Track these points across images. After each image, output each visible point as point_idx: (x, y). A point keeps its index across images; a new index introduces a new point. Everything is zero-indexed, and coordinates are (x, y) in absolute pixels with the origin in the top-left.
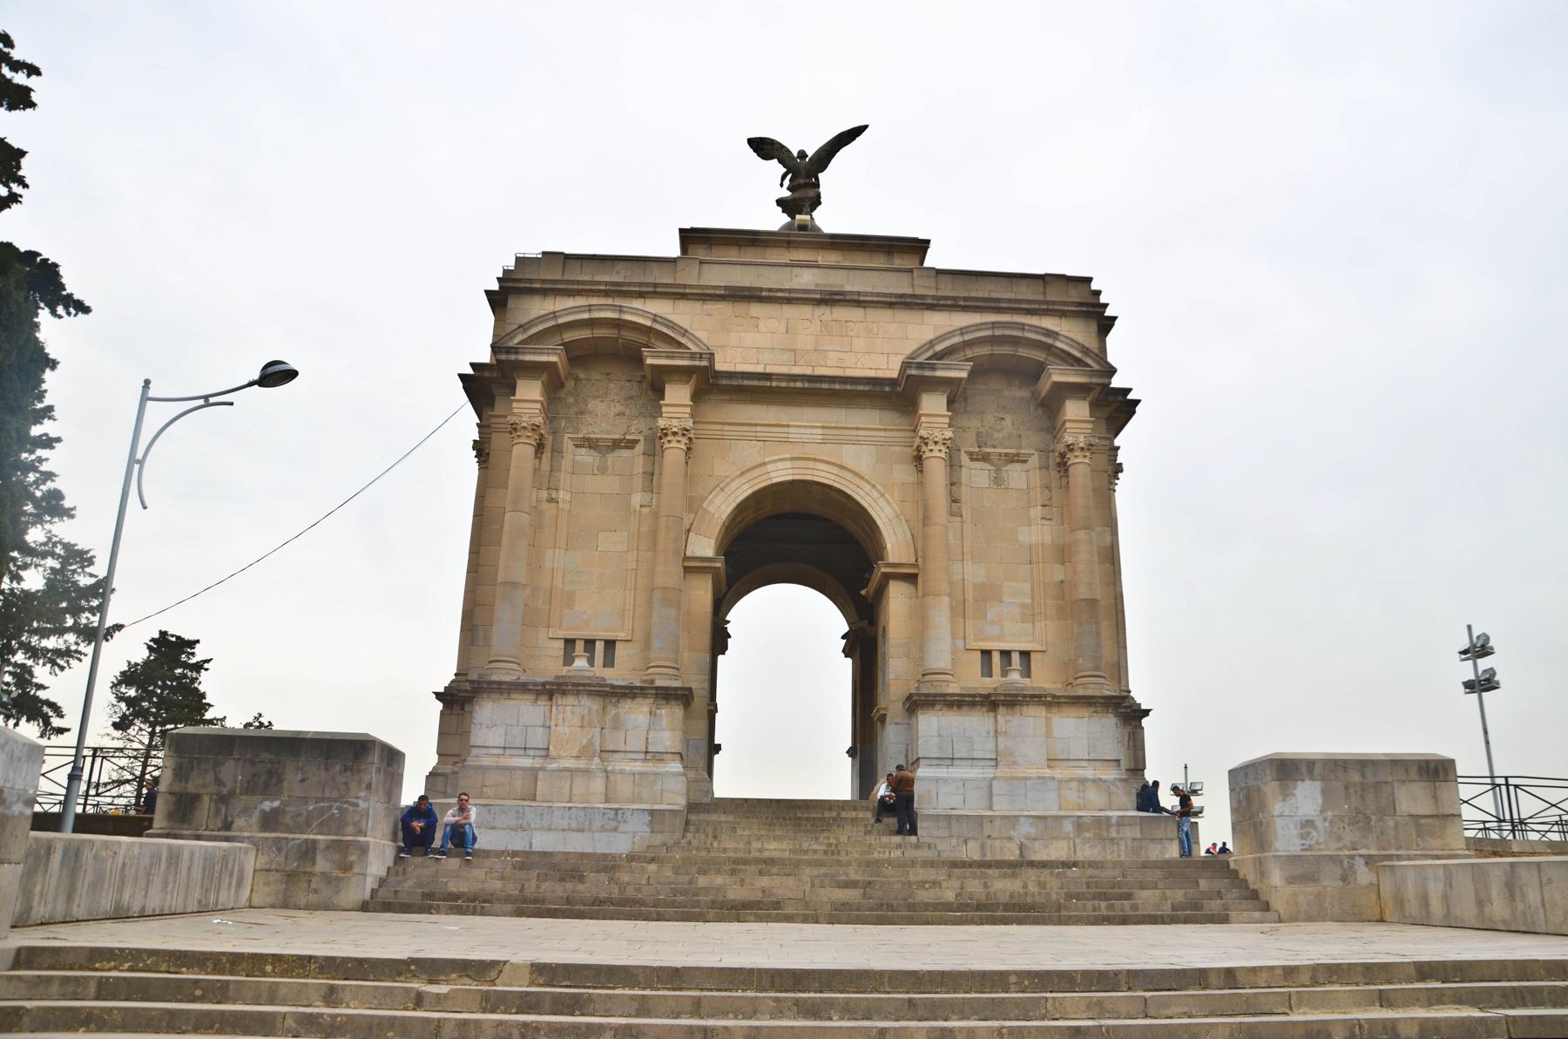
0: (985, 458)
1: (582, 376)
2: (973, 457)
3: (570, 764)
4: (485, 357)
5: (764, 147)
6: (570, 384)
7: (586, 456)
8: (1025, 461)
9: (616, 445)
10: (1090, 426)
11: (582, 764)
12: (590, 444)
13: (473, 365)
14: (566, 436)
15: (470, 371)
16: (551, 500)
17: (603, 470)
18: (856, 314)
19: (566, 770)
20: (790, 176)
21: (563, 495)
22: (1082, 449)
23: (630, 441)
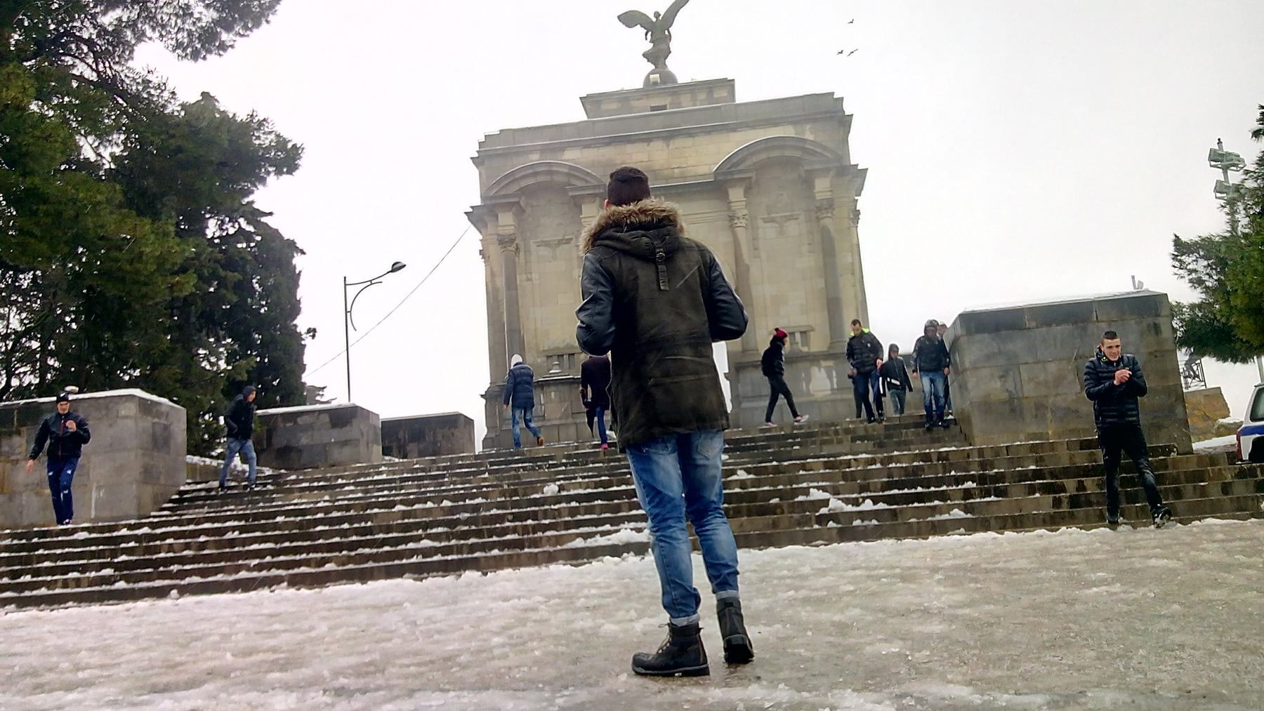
0: (773, 220)
1: (535, 204)
2: (766, 221)
3: (557, 422)
4: (478, 202)
5: (629, 19)
6: (528, 210)
7: (544, 251)
8: (796, 219)
9: (560, 243)
10: (829, 193)
11: (563, 422)
12: (546, 244)
13: (472, 207)
14: (531, 242)
15: (471, 210)
16: (528, 280)
17: (554, 258)
18: (688, 142)
19: (555, 425)
20: (650, 33)
21: (535, 276)
22: (826, 209)
23: (568, 239)
